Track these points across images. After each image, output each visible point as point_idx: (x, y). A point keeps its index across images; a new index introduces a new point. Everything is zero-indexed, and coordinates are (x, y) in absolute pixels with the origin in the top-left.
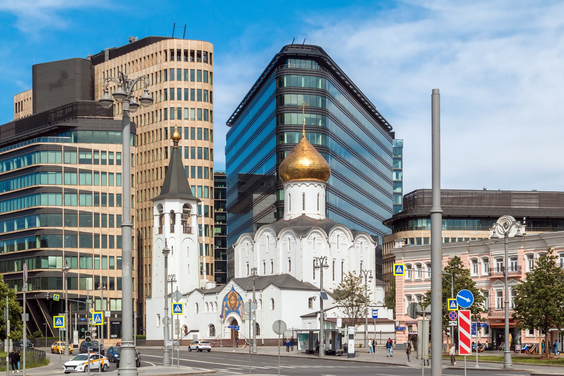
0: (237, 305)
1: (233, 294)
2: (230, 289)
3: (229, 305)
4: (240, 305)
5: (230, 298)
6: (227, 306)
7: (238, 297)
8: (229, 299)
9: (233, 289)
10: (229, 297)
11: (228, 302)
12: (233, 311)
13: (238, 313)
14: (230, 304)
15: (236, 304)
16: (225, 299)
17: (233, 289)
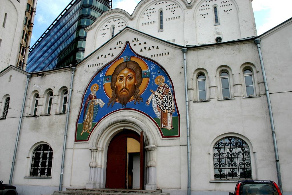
0: (142, 88)
1: (126, 65)
2: (117, 53)
3: (110, 92)
4: (152, 87)
5: (116, 73)
6: (100, 95)
7: (145, 69)
8: (112, 79)
9: (128, 48)
10: (110, 71)
11: (107, 84)
12: (125, 105)
13: (148, 112)
14: (115, 89)
15: (135, 87)
16: (94, 80)
17: (128, 48)
